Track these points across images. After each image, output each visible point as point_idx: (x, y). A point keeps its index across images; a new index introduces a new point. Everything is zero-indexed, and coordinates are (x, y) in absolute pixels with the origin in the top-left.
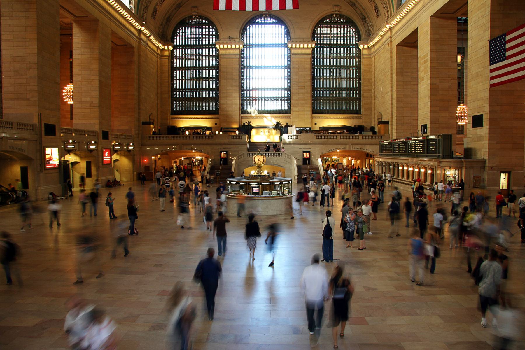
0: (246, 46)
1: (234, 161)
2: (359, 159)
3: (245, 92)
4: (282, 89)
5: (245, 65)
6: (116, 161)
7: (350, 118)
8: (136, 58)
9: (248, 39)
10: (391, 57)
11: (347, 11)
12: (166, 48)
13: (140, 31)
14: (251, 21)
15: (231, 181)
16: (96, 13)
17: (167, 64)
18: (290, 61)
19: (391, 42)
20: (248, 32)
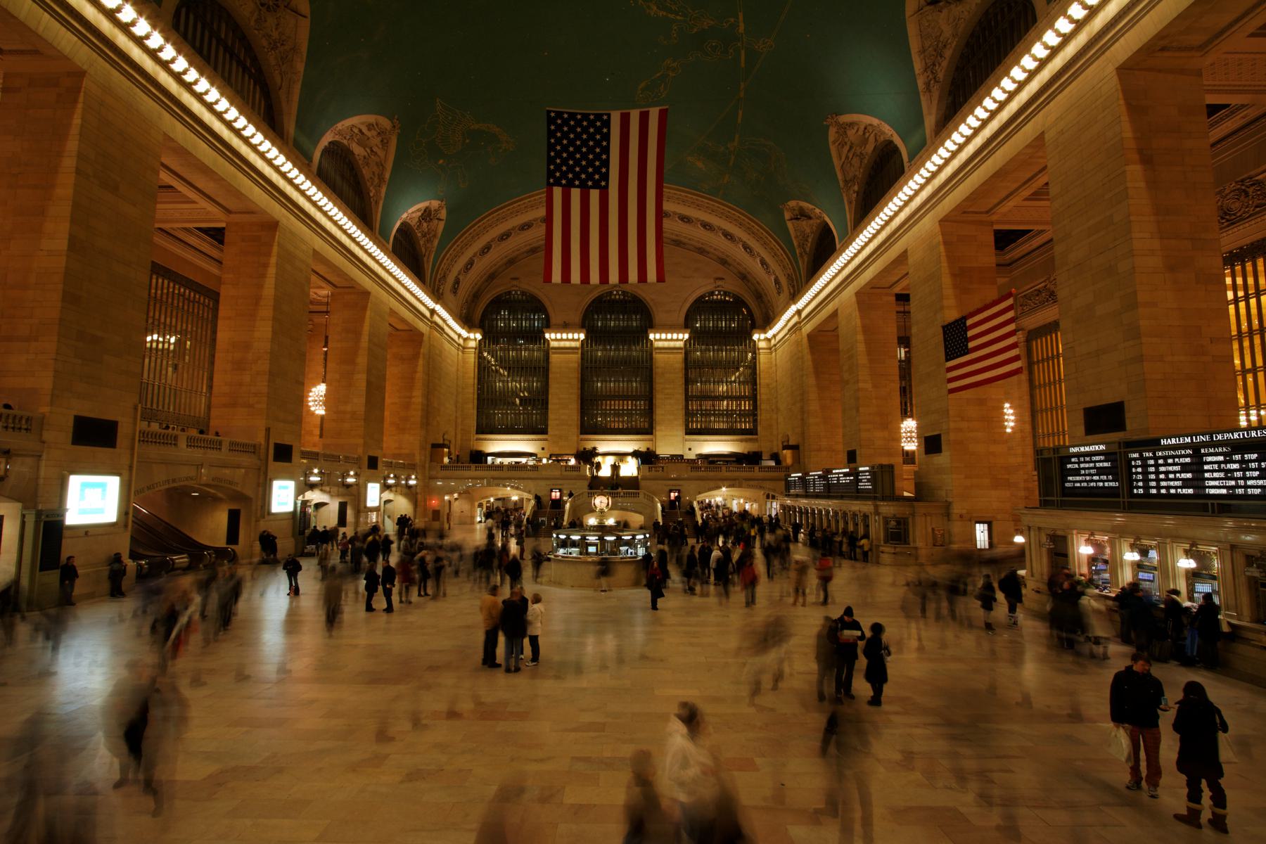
2: (755, 501)
6: (387, 502)
7: (741, 441)
12: (472, 336)
13: (433, 312)
16: (367, 283)
17: (472, 360)
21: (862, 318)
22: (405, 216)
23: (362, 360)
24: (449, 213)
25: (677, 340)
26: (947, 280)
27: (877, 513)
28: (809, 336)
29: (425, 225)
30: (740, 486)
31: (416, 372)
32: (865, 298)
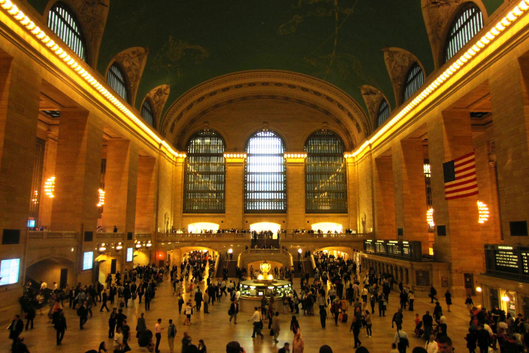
0: (249, 155)
1: (239, 257)
2: (347, 252)
3: (248, 194)
4: (279, 192)
5: (248, 171)
6: (136, 256)
8: (155, 168)
9: (251, 149)
10: (372, 167)
11: (333, 127)
12: (181, 155)
13: (160, 145)
14: (253, 135)
15: (243, 285)
16: (128, 135)
18: (286, 168)
19: (371, 155)
20: (251, 144)
21: (405, 154)
22: (148, 95)
23: (125, 178)
24: (171, 91)
25: (301, 158)
26: (446, 143)
27: (412, 268)
28: (376, 159)
29: (158, 97)
30: (338, 245)
31: (151, 180)
32: (407, 144)
